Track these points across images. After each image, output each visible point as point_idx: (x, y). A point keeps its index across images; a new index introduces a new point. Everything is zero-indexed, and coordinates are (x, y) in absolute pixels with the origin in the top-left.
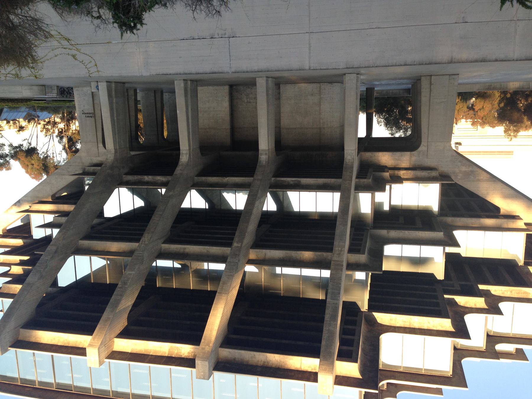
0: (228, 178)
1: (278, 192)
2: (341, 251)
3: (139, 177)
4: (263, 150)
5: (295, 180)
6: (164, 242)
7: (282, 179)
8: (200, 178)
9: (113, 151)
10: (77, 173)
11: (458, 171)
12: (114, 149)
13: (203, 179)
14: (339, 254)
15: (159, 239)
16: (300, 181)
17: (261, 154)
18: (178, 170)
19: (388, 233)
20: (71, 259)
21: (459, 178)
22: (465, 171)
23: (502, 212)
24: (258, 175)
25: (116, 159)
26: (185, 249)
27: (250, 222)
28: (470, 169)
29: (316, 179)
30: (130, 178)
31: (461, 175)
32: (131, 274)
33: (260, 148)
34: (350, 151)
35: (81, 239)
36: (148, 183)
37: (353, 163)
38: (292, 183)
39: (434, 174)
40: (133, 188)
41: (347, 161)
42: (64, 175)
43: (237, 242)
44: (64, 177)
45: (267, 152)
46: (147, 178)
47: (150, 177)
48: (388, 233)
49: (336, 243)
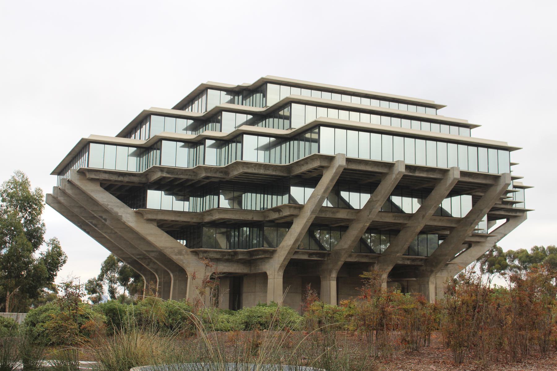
0: (355, 261)
1: (318, 249)
2: (309, 220)
3: (413, 263)
4: (334, 280)
5: (312, 258)
6: (406, 224)
7: (320, 259)
8: (373, 262)
9: (430, 283)
10: (452, 265)
11: (185, 255)
12: (428, 284)
13: (371, 261)
14: (311, 218)
15: (411, 227)
16: (309, 257)
17: (335, 277)
18: (390, 268)
19: (253, 218)
20: (463, 216)
21: (184, 251)
22: (181, 255)
23: (156, 224)
24: (340, 263)
25: (428, 277)
26: (395, 220)
27: (355, 236)
28: (177, 257)
29: (299, 258)
30: (419, 263)
31: (184, 253)
32: (431, 211)
33: (336, 282)
34: (280, 277)
35: (456, 227)
36: (408, 259)
37: (279, 270)
38: (314, 256)
39: (205, 255)
40: (418, 255)
41: (282, 271)
42: (462, 263)
43: (366, 225)
44: (462, 262)
45: (331, 279)
46: (408, 262)
47: (406, 263)
48: (253, 218)
49: (310, 224)
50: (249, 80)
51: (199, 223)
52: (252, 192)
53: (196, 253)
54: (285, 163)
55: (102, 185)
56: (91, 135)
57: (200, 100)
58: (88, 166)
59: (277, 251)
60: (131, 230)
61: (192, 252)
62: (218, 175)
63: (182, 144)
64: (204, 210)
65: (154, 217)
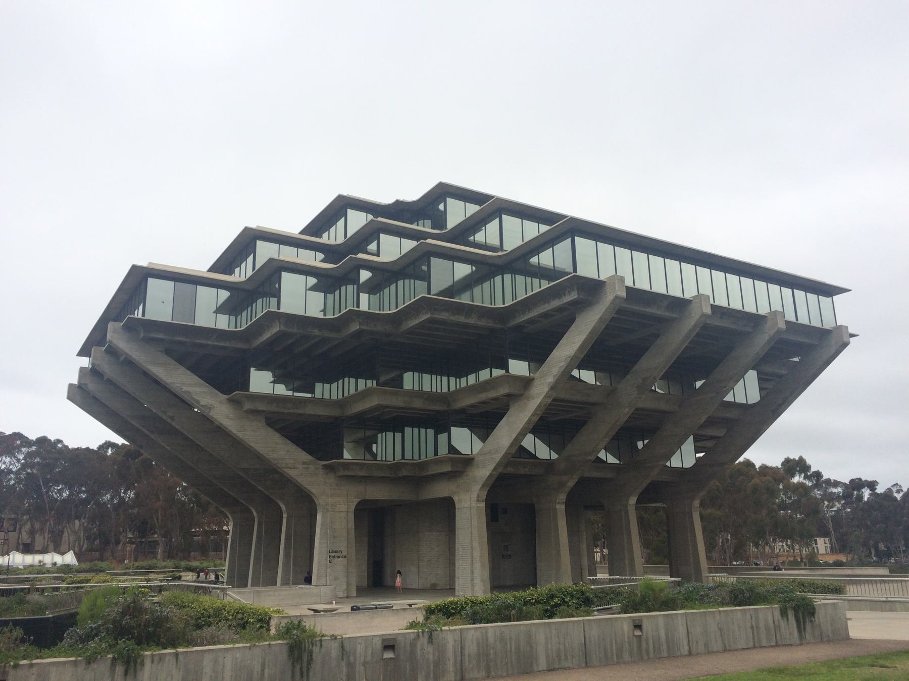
50: (413, 193)
51: (337, 418)
52: (414, 371)
53: (329, 469)
54: (504, 304)
55: (168, 352)
56: (150, 263)
57: (332, 230)
58: (143, 314)
59: (476, 459)
60: (219, 431)
61: (325, 467)
62: (380, 328)
63: (312, 281)
64: (346, 394)
65: (261, 407)
